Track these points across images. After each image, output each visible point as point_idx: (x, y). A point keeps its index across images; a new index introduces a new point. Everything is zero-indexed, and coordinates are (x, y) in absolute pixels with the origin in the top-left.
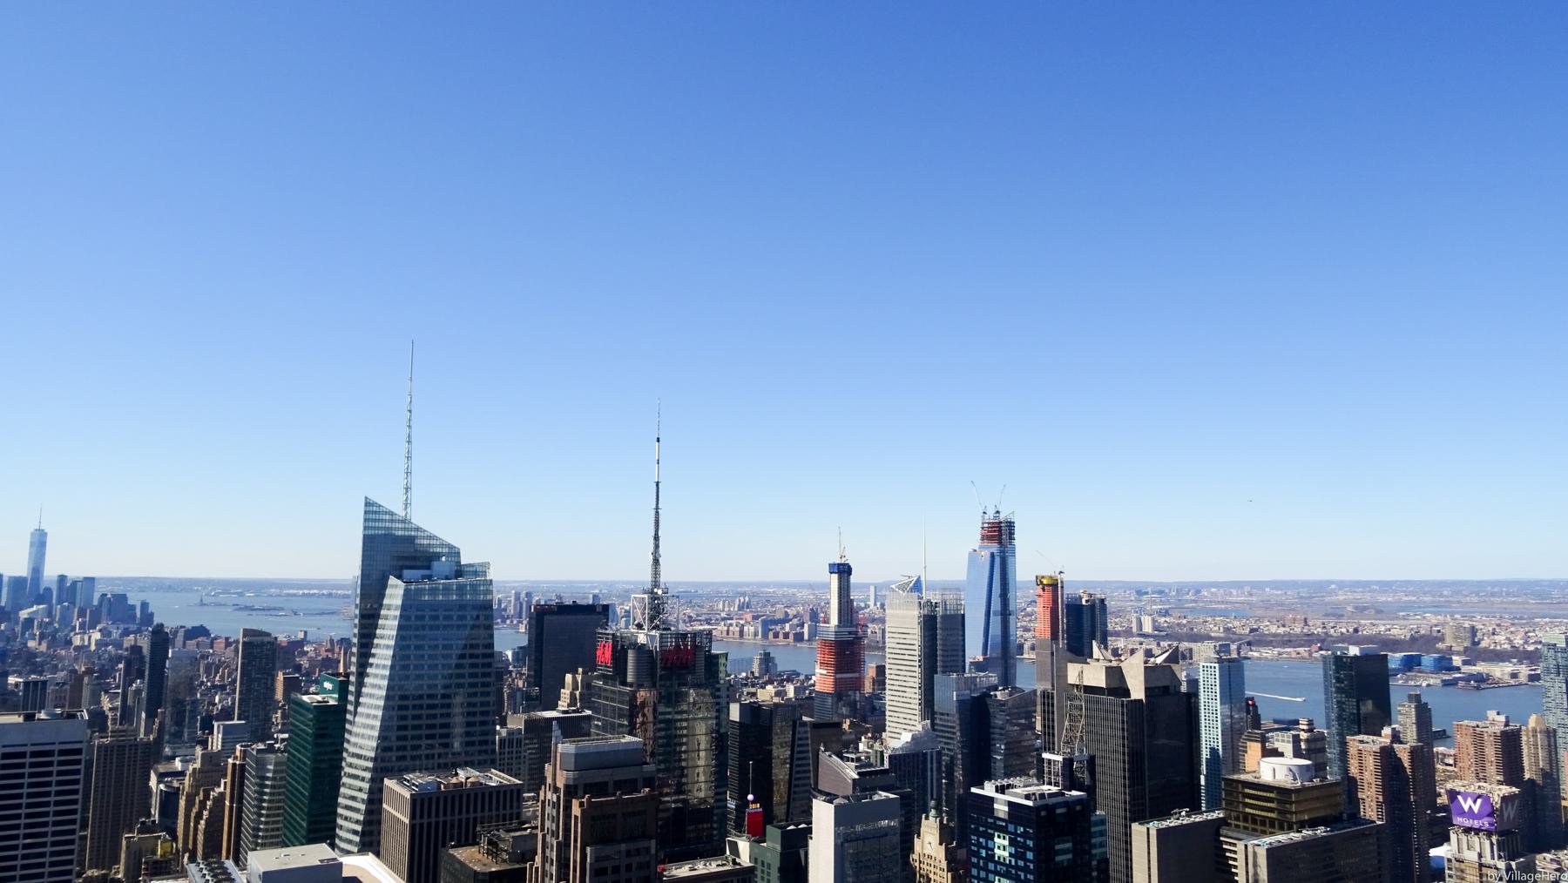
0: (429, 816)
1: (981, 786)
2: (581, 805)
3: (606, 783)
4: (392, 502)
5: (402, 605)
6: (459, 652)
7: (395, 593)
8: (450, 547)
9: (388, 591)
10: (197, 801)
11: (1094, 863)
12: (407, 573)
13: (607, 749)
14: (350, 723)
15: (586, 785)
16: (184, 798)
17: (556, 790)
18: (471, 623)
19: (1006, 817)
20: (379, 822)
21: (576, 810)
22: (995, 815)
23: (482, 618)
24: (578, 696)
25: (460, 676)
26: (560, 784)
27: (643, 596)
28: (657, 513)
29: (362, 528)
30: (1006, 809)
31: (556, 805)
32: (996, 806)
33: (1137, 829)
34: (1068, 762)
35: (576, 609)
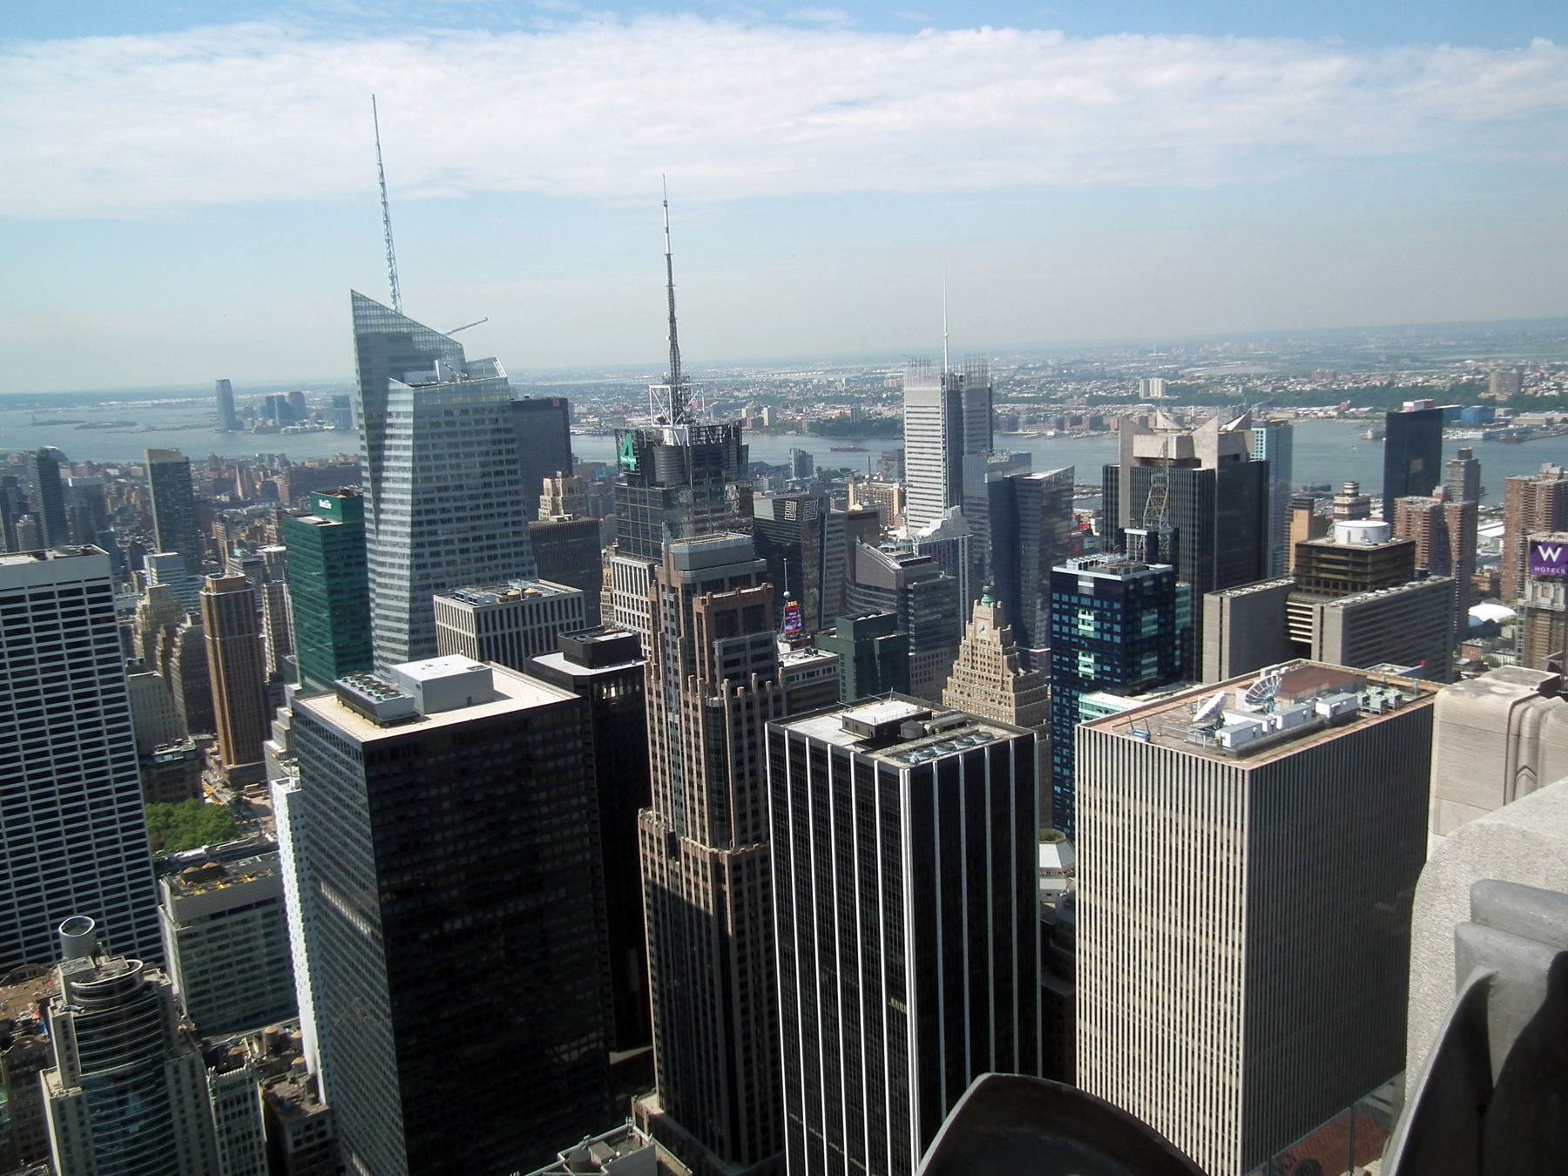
0: (494, 629)
1: (1063, 563)
2: (704, 602)
3: (722, 580)
4: (380, 294)
5: (415, 412)
6: (482, 459)
7: (402, 400)
8: (446, 341)
9: (391, 397)
10: (160, 637)
11: (1178, 632)
12: (409, 375)
13: (704, 549)
14: (373, 542)
15: (703, 583)
16: (139, 637)
17: (673, 590)
18: (491, 427)
19: (1092, 594)
20: (434, 640)
21: (698, 607)
22: (1080, 591)
23: (501, 421)
24: (560, 502)
25: (485, 485)
26: (677, 584)
27: (664, 387)
28: (671, 291)
29: (352, 327)
30: (1092, 585)
31: (673, 605)
32: (1080, 583)
33: (1210, 600)
34: (1152, 537)
35: (545, 404)
